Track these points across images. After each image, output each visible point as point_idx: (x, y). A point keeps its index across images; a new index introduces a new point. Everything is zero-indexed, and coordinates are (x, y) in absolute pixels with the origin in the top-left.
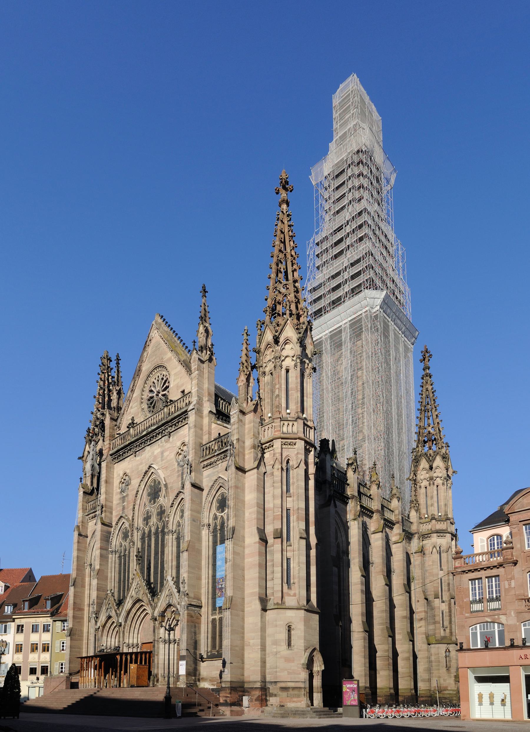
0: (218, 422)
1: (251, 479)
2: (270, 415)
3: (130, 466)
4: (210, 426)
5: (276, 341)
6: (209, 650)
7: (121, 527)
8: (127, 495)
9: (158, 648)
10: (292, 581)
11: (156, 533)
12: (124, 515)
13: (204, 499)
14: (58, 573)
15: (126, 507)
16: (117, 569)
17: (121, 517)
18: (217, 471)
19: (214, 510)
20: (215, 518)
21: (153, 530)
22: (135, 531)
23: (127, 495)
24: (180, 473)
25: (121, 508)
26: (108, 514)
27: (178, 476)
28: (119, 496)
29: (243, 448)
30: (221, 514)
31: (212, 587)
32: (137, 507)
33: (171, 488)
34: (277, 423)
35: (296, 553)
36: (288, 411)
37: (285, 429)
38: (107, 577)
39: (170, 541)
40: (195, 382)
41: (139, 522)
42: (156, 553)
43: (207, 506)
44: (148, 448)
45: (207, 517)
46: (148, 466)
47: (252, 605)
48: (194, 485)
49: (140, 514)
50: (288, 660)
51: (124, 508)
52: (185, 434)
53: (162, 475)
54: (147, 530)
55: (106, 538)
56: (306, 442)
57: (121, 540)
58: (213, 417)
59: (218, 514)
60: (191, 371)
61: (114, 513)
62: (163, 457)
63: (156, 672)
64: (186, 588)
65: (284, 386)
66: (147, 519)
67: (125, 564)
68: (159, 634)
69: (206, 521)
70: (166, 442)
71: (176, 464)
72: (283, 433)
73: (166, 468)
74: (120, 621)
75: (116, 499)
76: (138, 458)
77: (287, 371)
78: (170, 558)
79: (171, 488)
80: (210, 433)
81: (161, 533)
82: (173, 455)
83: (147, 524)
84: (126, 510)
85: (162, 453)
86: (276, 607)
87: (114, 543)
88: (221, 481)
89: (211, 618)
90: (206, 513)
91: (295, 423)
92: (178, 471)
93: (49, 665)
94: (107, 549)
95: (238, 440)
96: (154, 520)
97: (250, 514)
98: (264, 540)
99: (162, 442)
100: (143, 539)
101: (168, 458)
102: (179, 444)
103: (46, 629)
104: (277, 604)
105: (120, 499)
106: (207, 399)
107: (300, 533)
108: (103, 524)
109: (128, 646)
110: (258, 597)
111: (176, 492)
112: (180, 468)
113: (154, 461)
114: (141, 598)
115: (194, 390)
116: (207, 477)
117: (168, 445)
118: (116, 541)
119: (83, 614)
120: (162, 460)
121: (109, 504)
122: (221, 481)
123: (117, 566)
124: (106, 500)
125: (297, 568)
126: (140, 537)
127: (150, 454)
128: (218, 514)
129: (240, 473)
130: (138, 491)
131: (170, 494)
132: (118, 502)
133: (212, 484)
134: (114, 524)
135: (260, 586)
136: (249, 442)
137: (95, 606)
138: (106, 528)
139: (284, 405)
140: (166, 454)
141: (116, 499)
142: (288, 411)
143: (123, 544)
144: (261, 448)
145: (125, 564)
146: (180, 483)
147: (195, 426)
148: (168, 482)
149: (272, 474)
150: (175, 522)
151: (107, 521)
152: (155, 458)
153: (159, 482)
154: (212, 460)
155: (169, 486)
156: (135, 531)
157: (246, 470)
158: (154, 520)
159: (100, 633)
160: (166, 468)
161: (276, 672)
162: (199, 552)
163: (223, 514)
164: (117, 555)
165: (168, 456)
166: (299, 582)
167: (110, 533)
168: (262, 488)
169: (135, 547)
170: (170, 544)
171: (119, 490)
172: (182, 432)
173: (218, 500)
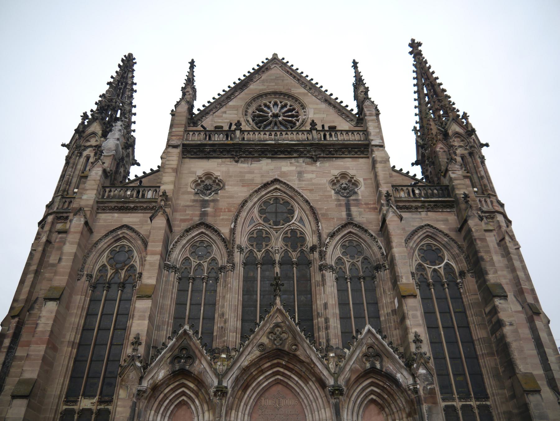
7: (193, 237)
8: (213, 201)
11: (286, 262)
18: (421, 218)
21: (277, 257)
22: (236, 250)
25: (198, 213)
30: (433, 267)
32: (240, 220)
33: (323, 215)
41: (242, 239)
51: (204, 214)
54: (259, 255)
66: (259, 238)
71: (333, 192)
73: (311, 190)
74: (225, 384)
82: (325, 181)
99: (298, 162)
100: (250, 263)
101: (314, 181)
102: (336, 172)
105: (194, 201)
118: (177, 256)
140: (307, 176)
143: (194, 262)
146: (344, 214)
152: (284, 174)
154: (414, 204)
156: (236, 250)
160: (311, 190)
163: (436, 267)
165: (311, 179)
172: (342, 163)
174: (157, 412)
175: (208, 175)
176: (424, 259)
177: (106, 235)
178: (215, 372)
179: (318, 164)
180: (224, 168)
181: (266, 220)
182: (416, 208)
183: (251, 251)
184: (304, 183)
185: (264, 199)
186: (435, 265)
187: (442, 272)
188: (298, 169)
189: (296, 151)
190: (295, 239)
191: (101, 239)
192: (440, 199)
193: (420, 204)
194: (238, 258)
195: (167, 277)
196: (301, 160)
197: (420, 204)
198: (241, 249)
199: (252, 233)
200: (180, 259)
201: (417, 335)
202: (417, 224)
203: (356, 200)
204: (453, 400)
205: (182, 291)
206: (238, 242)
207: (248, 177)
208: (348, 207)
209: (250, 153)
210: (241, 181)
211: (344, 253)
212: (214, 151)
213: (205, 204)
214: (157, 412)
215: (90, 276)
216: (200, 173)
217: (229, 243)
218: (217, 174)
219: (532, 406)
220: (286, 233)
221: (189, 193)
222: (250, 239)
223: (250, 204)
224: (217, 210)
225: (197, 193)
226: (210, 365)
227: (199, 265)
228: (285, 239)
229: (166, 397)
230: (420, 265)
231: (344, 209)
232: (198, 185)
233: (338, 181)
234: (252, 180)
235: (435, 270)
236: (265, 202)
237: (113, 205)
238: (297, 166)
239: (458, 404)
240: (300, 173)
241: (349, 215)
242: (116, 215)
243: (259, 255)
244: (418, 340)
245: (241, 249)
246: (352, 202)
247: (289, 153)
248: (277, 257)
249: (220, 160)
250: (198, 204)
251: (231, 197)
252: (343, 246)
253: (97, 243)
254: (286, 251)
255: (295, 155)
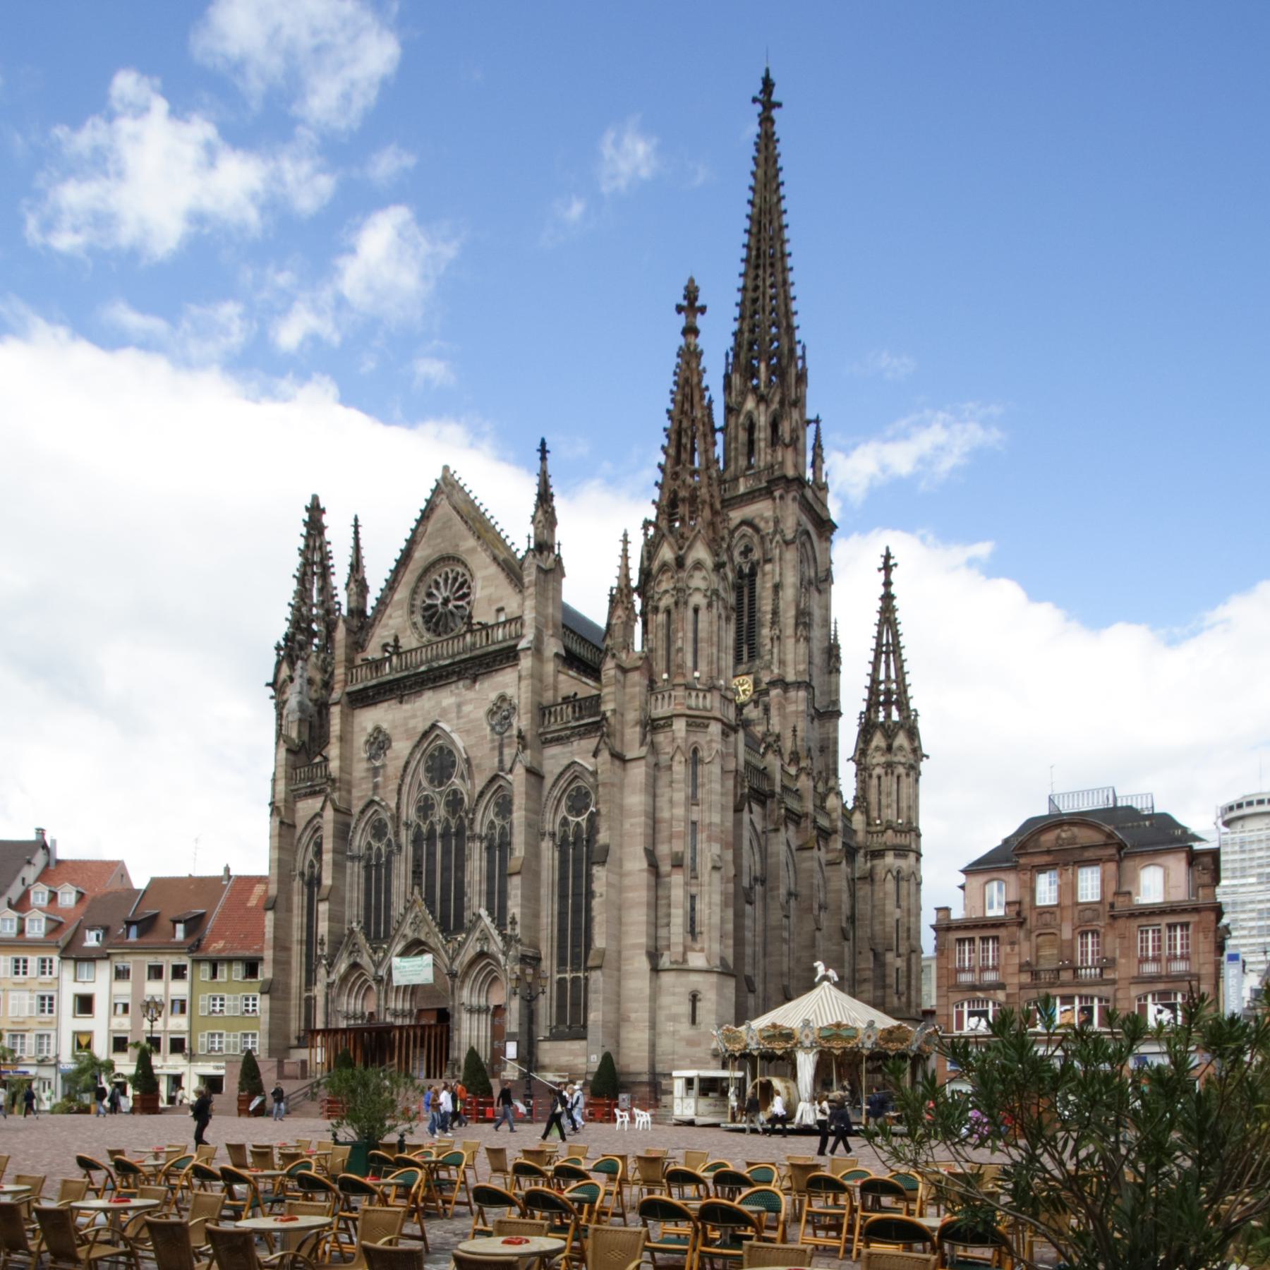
0: (571, 673)
1: (638, 772)
2: (665, 676)
3: (390, 717)
4: (556, 677)
5: (680, 562)
6: (554, 1024)
8: (384, 766)
9: (460, 1019)
10: (697, 930)
11: (445, 835)
12: (377, 798)
13: (545, 793)
14: (185, 874)
15: (381, 784)
16: (362, 886)
17: (372, 802)
19: (563, 811)
20: (565, 822)
21: (439, 829)
23: (384, 766)
24: (497, 744)
25: (371, 785)
26: (344, 793)
27: (493, 749)
28: (364, 765)
29: (622, 723)
31: (559, 930)
32: (405, 789)
33: (478, 766)
34: (680, 692)
35: (706, 888)
36: (697, 674)
37: (693, 702)
38: (343, 899)
39: (477, 851)
40: (530, 603)
41: (410, 813)
42: (446, 869)
43: (551, 803)
44: (428, 695)
45: (551, 823)
46: (428, 724)
47: (641, 963)
48: (530, 771)
49: (412, 801)
50: (691, 1043)
52: (508, 683)
53: (460, 743)
54: (424, 828)
55: (343, 833)
56: (724, 723)
57: (369, 839)
58: (558, 662)
59: (570, 818)
60: (522, 585)
61: (356, 793)
62: (461, 713)
63: (456, 1054)
64: (518, 930)
65: (690, 635)
66: (425, 807)
67: (378, 880)
68: (460, 997)
69: (548, 827)
70: (468, 688)
71: (489, 728)
72: (690, 708)
73: (468, 732)
74: (380, 973)
75: (360, 769)
76: (406, 707)
77: (696, 610)
78: (477, 877)
79: (478, 766)
80: (556, 689)
81: (458, 836)
82: (481, 713)
83: (425, 818)
84: (381, 791)
85: (459, 706)
86: (675, 967)
87: (356, 843)
88: (577, 768)
89: (557, 976)
90: (549, 816)
91: (708, 696)
92: (493, 741)
93: (186, 1036)
94: (343, 853)
95: (614, 711)
96: (440, 812)
97: (636, 825)
98: (654, 866)
100: (417, 841)
101: (472, 716)
102: (493, 696)
103: (178, 972)
104: (676, 962)
105: (368, 770)
106: (550, 632)
107: (713, 860)
108: (336, 810)
109: (395, 1014)
110: (644, 951)
111: (488, 775)
112: (497, 737)
113: (440, 715)
114: (423, 939)
115: (529, 616)
116: (555, 759)
117: (470, 695)
118: (359, 841)
119: (290, 957)
120: (459, 718)
121: (346, 777)
122: (577, 768)
123: (362, 880)
124: (341, 769)
125: (707, 912)
126: (411, 837)
127: (433, 703)
128: (570, 818)
129: (617, 763)
130: (407, 763)
131: (476, 776)
132: (364, 774)
133: (560, 769)
134: (356, 810)
135: (648, 935)
136: (632, 715)
137: (326, 948)
138: (341, 817)
139: (690, 663)
140: (467, 709)
141: (360, 769)
142: (697, 674)
143: (375, 845)
144: (652, 726)
145: (378, 880)
146: (496, 760)
147: (532, 676)
148: (471, 755)
149: (670, 768)
150: (486, 822)
151: (342, 806)
152: (444, 712)
153: (450, 753)
154: (563, 733)
155: (474, 762)
157: (628, 757)
158: (440, 812)
159: (335, 991)
160: (468, 732)
161: (673, 1060)
162: (537, 875)
163: (579, 819)
164: (363, 863)
166: (709, 931)
167: (348, 825)
168: (652, 789)
169: (403, 853)
170: (477, 856)
171: (365, 756)
173: (569, 797)
174: (349, 996)
175: (378, 729)
176: (571, 809)
177: (306, 828)
178: (373, 961)
179: (477, 686)
180: (390, 717)
181: (431, 781)
182: (568, 737)
183: (419, 826)
184: (462, 721)
185: (428, 752)
186: (578, 815)
187: (584, 825)
188: (458, 700)
189: (454, 672)
190: (455, 802)
191: (302, 834)
192: (590, 720)
193: (568, 732)
194: (405, 837)
195: (352, 868)
196: (461, 684)
197: (568, 732)
198: (408, 826)
199: (419, 801)
200: (363, 844)
201: (513, 918)
202: (566, 762)
203: (510, 737)
204: (566, 972)
205: (368, 879)
206: (404, 818)
207: (412, 723)
208: (501, 747)
209: (411, 687)
210: (407, 731)
211: (497, 815)
212: (379, 693)
213: (375, 771)
214: (349, 996)
215: (302, 874)
216: (370, 729)
217: (396, 818)
218: (385, 726)
219: (591, 982)
220: (448, 795)
221: (360, 760)
222: (419, 809)
223: (413, 764)
224: (386, 778)
225: (369, 759)
226: (371, 957)
227: (379, 849)
228: (448, 804)
229: (354, 984)
230: (565, 819)
231: (496, 753)
232: (372, 744)
233: (499, 708)
234: (415, 728)
235: (578, 824)
236: (432, 756)
237: (303, 791)
238: (459, 695)
239: (568, 976)
240: (459, 706)
241: (501, 761)
242: (310, 801)
243: (424, 828)
244: (513, 922)
245: (408, 826)
246: (506, 741)
247: (447, 677)
248: (439, 829)
249: (385, 705)
250: (370, 774)
251: (397, 758)
252: (497, 804)
253: (300, 838)
254: (447, 820)
255: (455, 678)
